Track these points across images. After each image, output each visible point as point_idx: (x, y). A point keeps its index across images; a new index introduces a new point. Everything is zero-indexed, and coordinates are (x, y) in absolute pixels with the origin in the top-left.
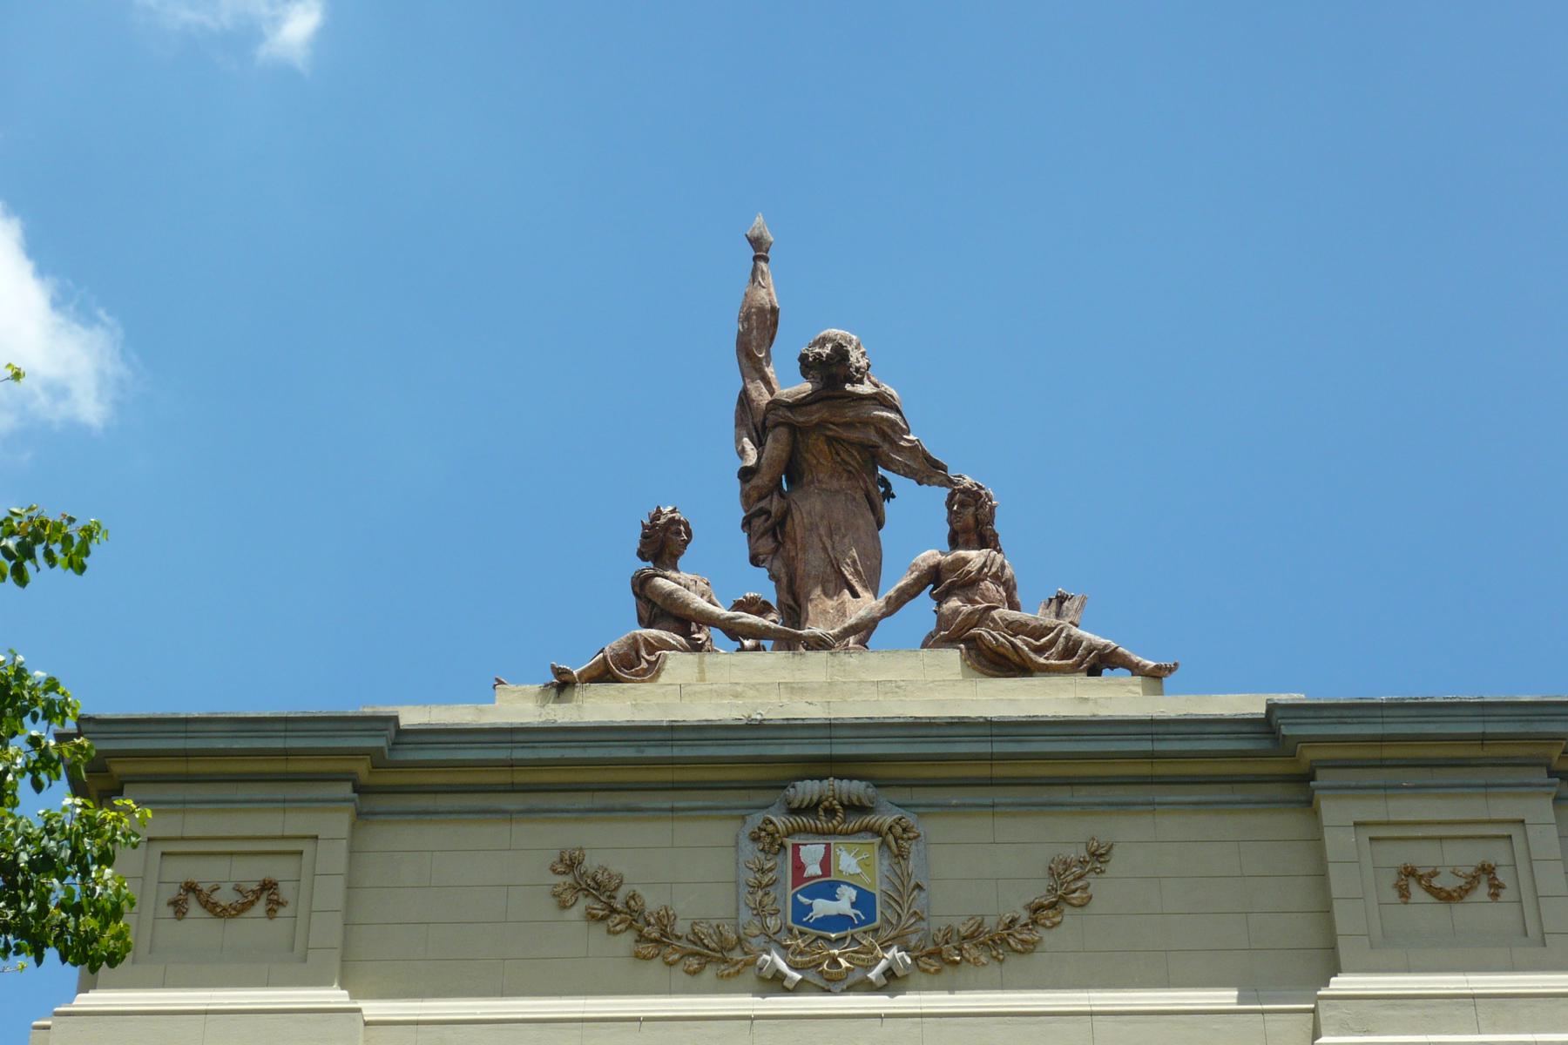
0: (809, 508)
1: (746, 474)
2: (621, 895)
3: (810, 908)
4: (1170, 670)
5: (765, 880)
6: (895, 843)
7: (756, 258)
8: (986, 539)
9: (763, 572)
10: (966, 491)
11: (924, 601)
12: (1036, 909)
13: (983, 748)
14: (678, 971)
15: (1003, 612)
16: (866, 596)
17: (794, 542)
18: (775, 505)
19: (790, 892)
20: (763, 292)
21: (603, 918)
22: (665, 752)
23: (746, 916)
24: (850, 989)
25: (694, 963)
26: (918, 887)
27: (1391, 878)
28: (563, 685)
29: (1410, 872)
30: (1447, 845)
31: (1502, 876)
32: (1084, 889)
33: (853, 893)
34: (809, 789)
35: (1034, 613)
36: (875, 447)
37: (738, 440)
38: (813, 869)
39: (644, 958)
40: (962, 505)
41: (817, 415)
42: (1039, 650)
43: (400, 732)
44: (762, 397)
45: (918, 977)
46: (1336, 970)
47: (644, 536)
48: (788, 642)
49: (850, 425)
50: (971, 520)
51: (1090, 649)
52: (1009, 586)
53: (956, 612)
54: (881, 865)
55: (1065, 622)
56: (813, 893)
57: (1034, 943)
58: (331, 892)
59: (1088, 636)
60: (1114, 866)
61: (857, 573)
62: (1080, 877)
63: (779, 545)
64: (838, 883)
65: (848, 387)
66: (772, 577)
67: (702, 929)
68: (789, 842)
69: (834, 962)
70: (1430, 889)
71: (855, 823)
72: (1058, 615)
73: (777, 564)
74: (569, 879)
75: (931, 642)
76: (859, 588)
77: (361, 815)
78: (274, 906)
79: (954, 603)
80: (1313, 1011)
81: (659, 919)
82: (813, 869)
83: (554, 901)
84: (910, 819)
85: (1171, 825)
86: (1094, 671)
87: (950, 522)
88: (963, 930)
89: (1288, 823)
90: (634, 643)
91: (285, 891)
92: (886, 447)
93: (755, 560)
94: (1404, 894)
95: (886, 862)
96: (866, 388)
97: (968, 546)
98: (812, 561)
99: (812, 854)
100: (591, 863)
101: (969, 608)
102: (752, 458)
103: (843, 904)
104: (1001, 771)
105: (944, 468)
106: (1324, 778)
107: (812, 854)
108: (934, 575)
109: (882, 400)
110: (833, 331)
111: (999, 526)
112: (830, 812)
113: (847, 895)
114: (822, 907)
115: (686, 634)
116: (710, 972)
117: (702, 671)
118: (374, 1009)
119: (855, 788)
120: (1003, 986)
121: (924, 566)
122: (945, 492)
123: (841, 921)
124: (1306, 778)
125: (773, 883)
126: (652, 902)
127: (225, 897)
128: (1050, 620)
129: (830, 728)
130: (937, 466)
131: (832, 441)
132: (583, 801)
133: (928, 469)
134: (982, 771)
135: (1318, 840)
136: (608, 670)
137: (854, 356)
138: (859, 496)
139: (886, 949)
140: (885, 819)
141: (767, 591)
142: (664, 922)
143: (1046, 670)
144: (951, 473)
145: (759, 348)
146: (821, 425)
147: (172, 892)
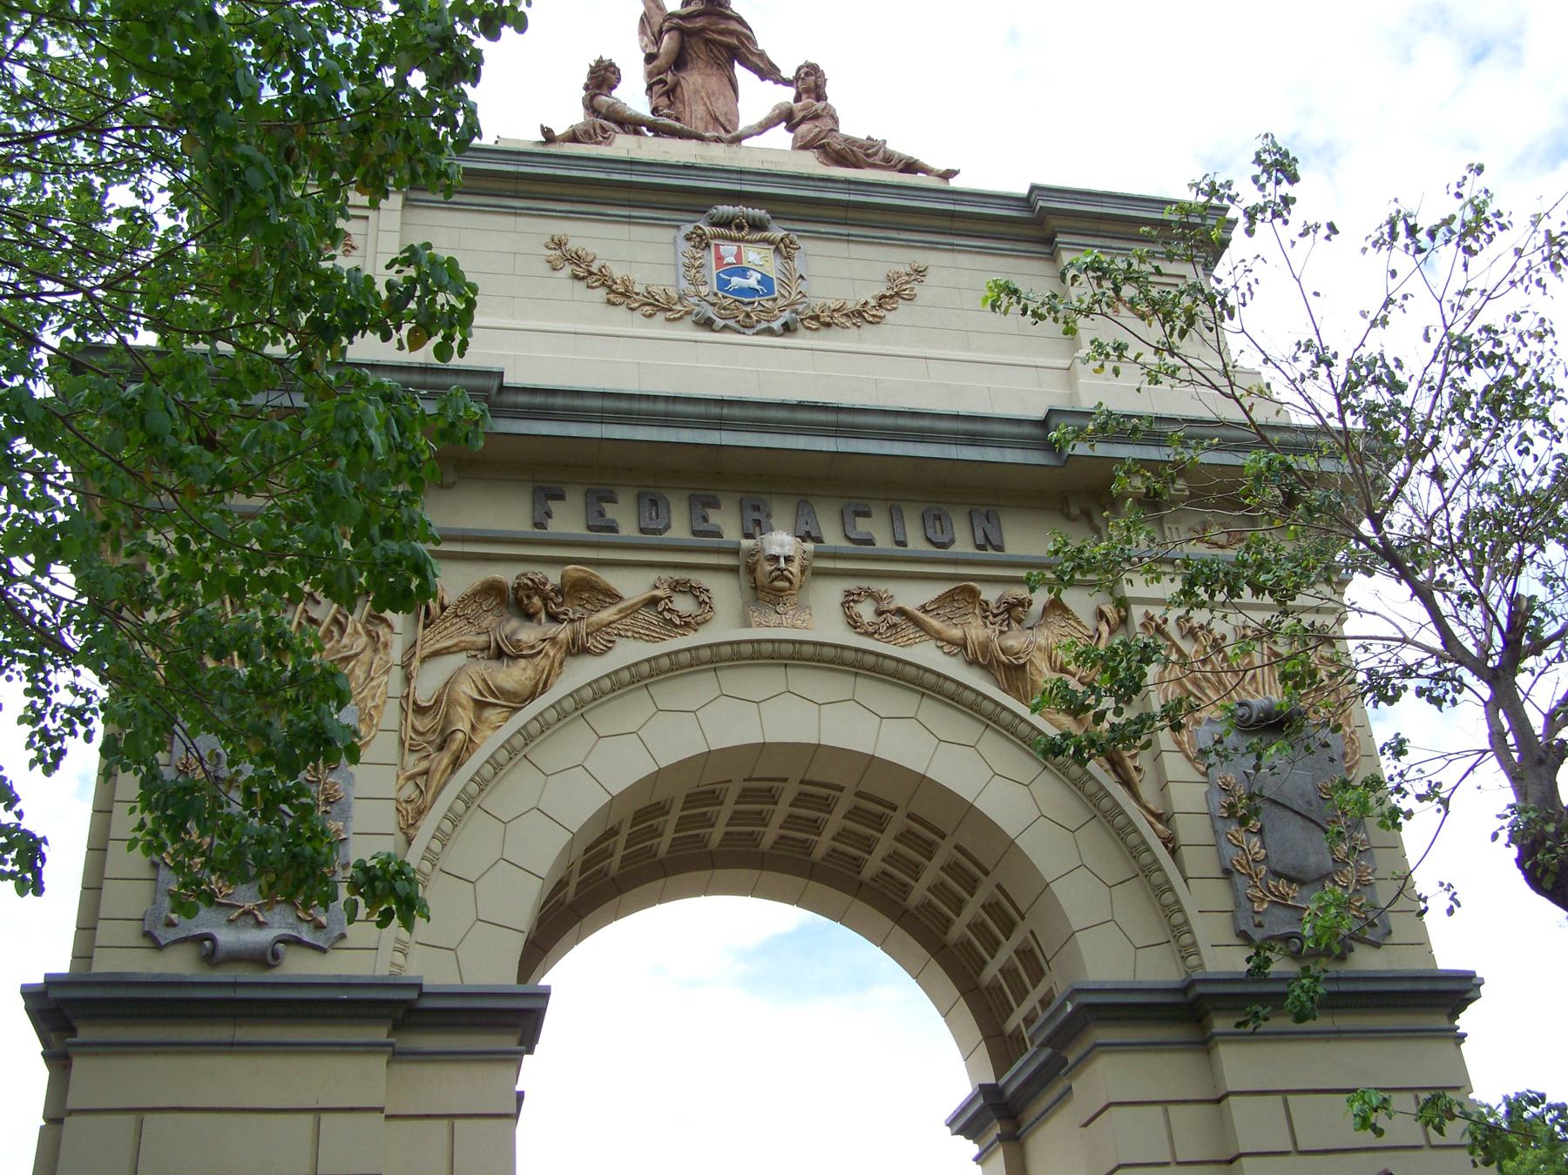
1: (650, 58)
5: (697, 264)
6: (783, 249)
8: (820, 96)
14: (638, 314)
19: (715, 272)
21: (583, 278)
25: (648, 309)
26: (801, 277)
32: (912, 290)
33: (759, 276)
34: (726, 210)
39: (614, 304)
45: (802, 330)
49: (722, 33)
50: (813, 85)
60: (929, 279)
67: (653, 289)
68: (713, 242)
71: (757, 236)
74: (558, 252)
81: (623, 281)
83: (548, 265)
84: (793, 236)
85: (963, 260)
88: (833, 307)
100: (573, 245)
103: (752, 281)
107: (729, 251)
112: (740, 228)
114: (736, 281)
119: (759, 213)
123: (752, 291)
125: (701, 266)
126: (617, 272)
146: (703, 30)
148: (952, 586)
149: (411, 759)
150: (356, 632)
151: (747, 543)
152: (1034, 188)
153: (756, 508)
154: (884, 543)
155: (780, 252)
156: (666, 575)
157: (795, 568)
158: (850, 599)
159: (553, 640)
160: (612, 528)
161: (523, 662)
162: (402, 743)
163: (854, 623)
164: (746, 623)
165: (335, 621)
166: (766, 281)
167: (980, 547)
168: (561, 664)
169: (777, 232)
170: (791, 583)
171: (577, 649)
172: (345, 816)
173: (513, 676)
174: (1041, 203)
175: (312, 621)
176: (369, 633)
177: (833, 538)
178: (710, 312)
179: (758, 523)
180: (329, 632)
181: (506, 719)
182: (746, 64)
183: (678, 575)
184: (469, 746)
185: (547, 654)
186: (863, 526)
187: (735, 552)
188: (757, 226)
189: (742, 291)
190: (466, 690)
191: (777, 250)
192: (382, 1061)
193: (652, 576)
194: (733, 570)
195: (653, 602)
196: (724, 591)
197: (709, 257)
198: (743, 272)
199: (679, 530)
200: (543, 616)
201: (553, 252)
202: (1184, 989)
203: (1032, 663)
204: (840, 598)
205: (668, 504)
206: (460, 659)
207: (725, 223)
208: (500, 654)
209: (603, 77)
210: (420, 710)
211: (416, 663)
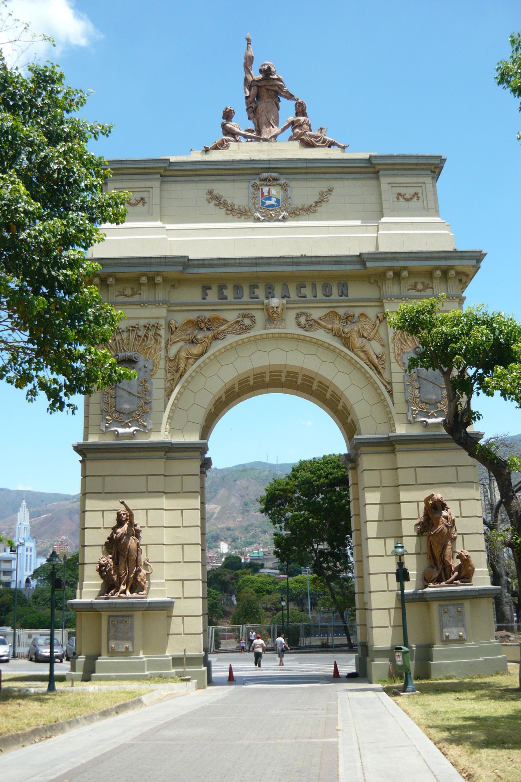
0: (262, 106)
1: (247, 98)
2: (222, 200)
3: (265, 203)
4: (347, 147)
5: (255, 196)
6: (284, 187)
7: (248, 44)
8: (304, 114)
9: (251, 122)
10: (300, 103)
11: (290, 129)
12: (316, 203)
13: (305, 165)
14: (236, 217)
15: (309, 132)
16: (276, 127)
17: (259, 114)
18: (254, 105)
19: (261, 199)
20: (250, 52)
22: (232, 167)
23: (251, 204)
24: (275, 221)
25: (239, 215)
26: (290, 198)
27: (396, 195)
28: (207, 150)
29: (399, 194)
30: (408, 188)
31: (420, 195)
33: (275, 199)
34: (265, 175)
35: (315, 133)
36: (278, 91)
37: (245, 89)
38: (266, 194)
40: (299, 106)
41: (263, 83)
42: (317, 142)
43: (170, 163)
44: (251, 79)
45: (290, 218)
46: (383, 216)
47: (224, 114)
48: (258, 139)
49: (271, 86)
50: (301, 110)
51: (329, 141)
52: (310, 126)
53: (298, 132)
54: (281, 193)
55: (322, 135)
56: (266, 199)
57: (316, 210)
58: (157, 200)
59: (329, 138)
60: (334, 192)
61: (274, 122)
62: (326, 195)
63: (255, 115)
64: (272, 197)
65: (271, 77)
66: (254, 123)
68: (260, 187)
69: (271, 215)
70: (404, 198)
71: (275, 183)
72: (321, 133)
73: (255, 120)
74: (210, 196)
75: (291, 139)
76: (274, 126)
77: (162, 182)
78: (144, 203)
79: (297, 130)
80: (377, 226)
81: (231, 206)
82: (266, 194)
83: (207, 201)
84: (288, 182)
85: (346, 183)
86: (329, 147)
87: (296, 110)
88: (300, 208)
89: (373, 183)
90: (223, 140)
91: (146, 200)
92: (280, 91)
93: (249, 119)
94: (398, 199)
95: (282, 192)
96: (275, 77)
97: (300, 116)
98: (263, 119)
99: (266, 190)
100: (215, 192)
101: (300, 131)
102: (248, 94)
103: (273, 202)
104: (308, 171)
105: (294, 96)
106: (381, 173)
107: (266, 190)
108: (292, 123)
109: (279, 79)
110: (267, 62)
111: (307, 111)
112: (270, 180)
113: (274, 200)
114: (268, 202)
115: (235, 138)
116: (243, 217)
117: (239, 147)
118: (168, 226)
119: (275, 175)
120: (309, 220)
121: (290, 121)
122: (295, 102)
123: (272, 206)
124: (378, 172)
125: (257, 197)
126: (229, 201)
127: (133, 201)
128: (319, 134)
129: (269, 161)
130: (292, 96)
131: (267, 90)
132: (213, 178)
133: (290, 96)
134: (304, 171)
135: (379, 187)
136: (217, 147)
137: (272, 68)
138: (274, 103)
139: (282, 212)
140: (282, 182)
141: (252, 126)
142: (232, 206)
143: (319, 146)
144: (295, 97)
145: (249, 66)
146: (265, 86)
148: (327, 311)
149: (169, 375)
150: (151, 339)
154: (309, 297)
158: (298, 316)
159: (208, 337)
160: (225, 298)
161: (199, 345)
162: (166, 370)
163: (299, 325)
165: (145, 336)
167: (341, 296)
168: (211, 344)
171: (215, 338)
172: (150, 395)
173: (196, 350)
175: (139, 336)
176: (155, 339)
180: (143, 340)
181: (195, 362)
182: (281, 95)
183: (245, 312)
184: (185, 371)
185: (206, 342)
186: (303, 291)
189: (270, 206)
190: (183, 354)
193: (237, 313)
195: (238, 322)
196: (260, 317)
198: (270, 199)
200: (205, 329)
201: (208, 196)
203: (351, 336)
204: (295, 316)
205: (243, 288)
206: (182, 343)
208: (193, 342)
209: (228, 115)
210: (170, 361)
211: (169, 346)
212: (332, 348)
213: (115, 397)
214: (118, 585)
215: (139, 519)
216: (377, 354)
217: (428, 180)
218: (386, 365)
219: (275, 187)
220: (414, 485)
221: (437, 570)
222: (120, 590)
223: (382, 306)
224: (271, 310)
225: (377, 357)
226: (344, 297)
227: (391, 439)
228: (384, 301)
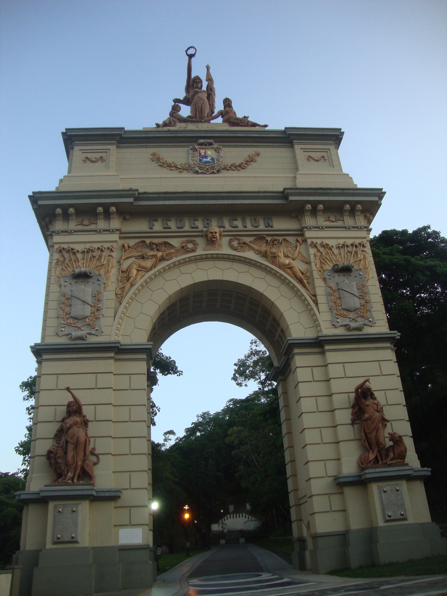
3: (202, 160)
6: (217, 150)
19: (199, 158)
24: (210, 174)
26: (222, 157)
31: (326, 158)
33: (211, 158)
34: (201, 141)
68: (198, 150)
84: (221, 147)
99: (202, 152)
103: (209, 159)
106: (294, 141)
107: (202, 152)
112: (206, 145)
114: (204, 160)
123: (209, 162)
135: (294, 152)
147: (84, 159)
151: (205, 229)
152: (286, 128)
153: (208, 220)
154: (241, 227)
155: (216, 151)
156: (184, 239)
157: (218, 235)
164: (205, 250)
166: (213, 159)
167: (267, 227)
169: (216, 145)
170: (217, 239)
174: (288, 132)
177: (228, 227)
178: (197, 169)
179: (208, 224)
186: (235, 223)
187: (202, 231)
188: (210, 144)
189: (206, 162)
191: (216, 150)
192: (112, 361)
194: (202, 236)
197: (197, 154)
198: (206, 157)
199: (187, 228)
202: (317, 338)
207: (201, 144)
212: (263, 266)
213: (71, 306)
214: (66, 472)
215: (87, 411)
216: (302, 271)
217: (332, 148)
218: (310, 280)
219: (210, 149)
220: (343, 378)
221: (373, 452)
222: (67, 478)
223: (302, 235)
224: (210, 235)
225: (302, 273)
226: (270, 228)
227: (320, 338)
228: (305, 229)
